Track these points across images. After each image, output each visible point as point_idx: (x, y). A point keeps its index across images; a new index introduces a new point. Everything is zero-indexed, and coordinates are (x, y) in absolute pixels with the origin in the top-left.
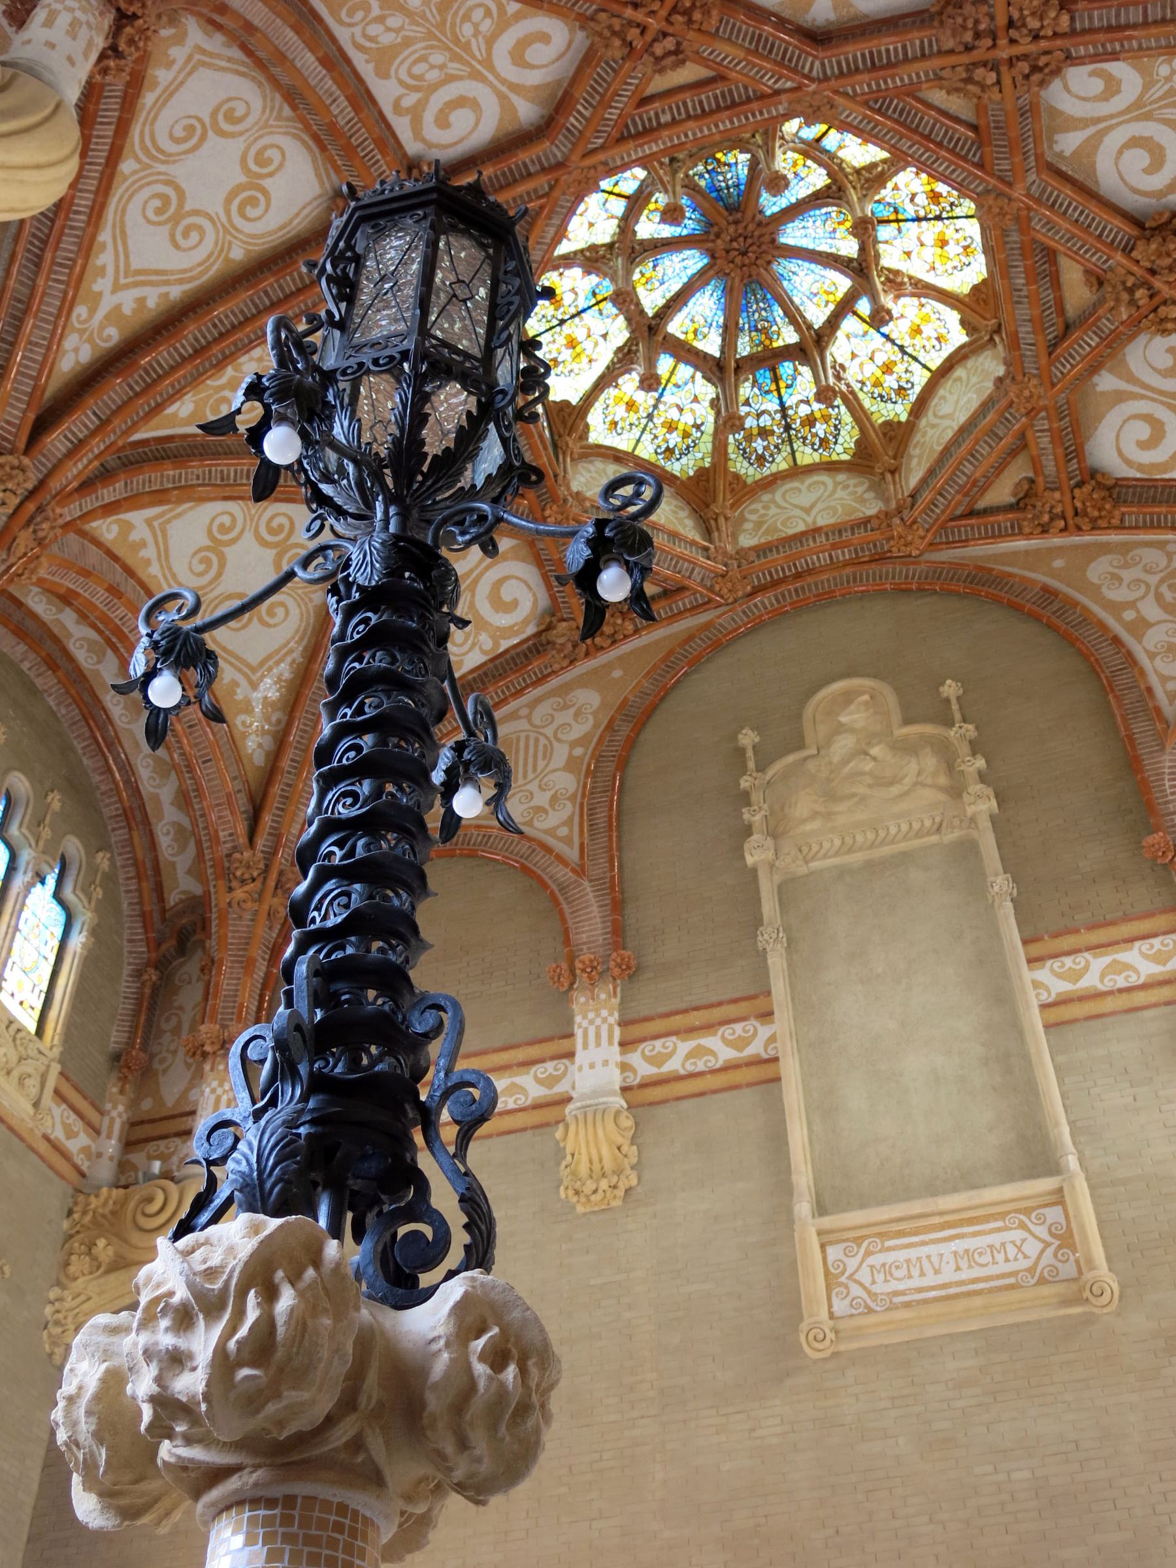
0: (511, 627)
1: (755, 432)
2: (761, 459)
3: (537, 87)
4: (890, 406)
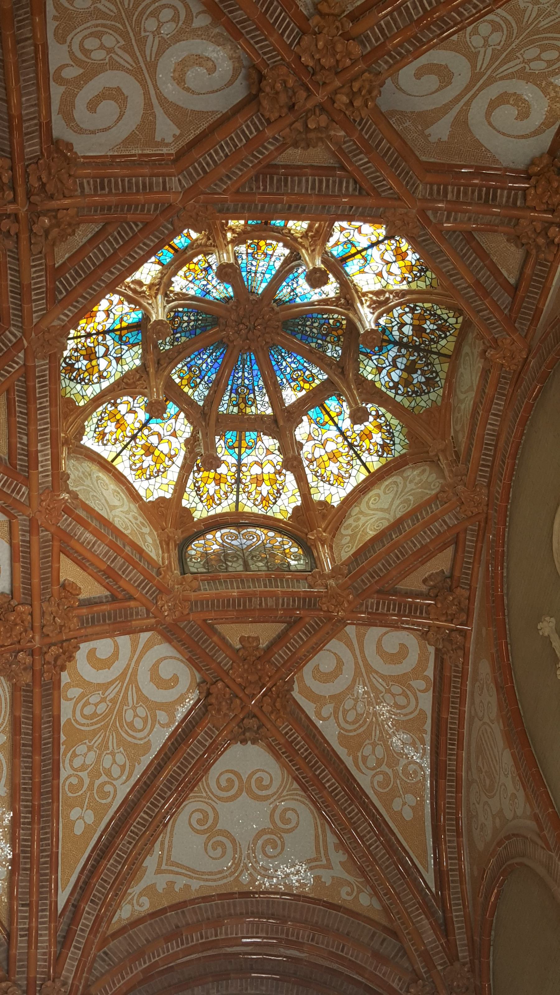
0: (420, 660)
1: (405, 375)
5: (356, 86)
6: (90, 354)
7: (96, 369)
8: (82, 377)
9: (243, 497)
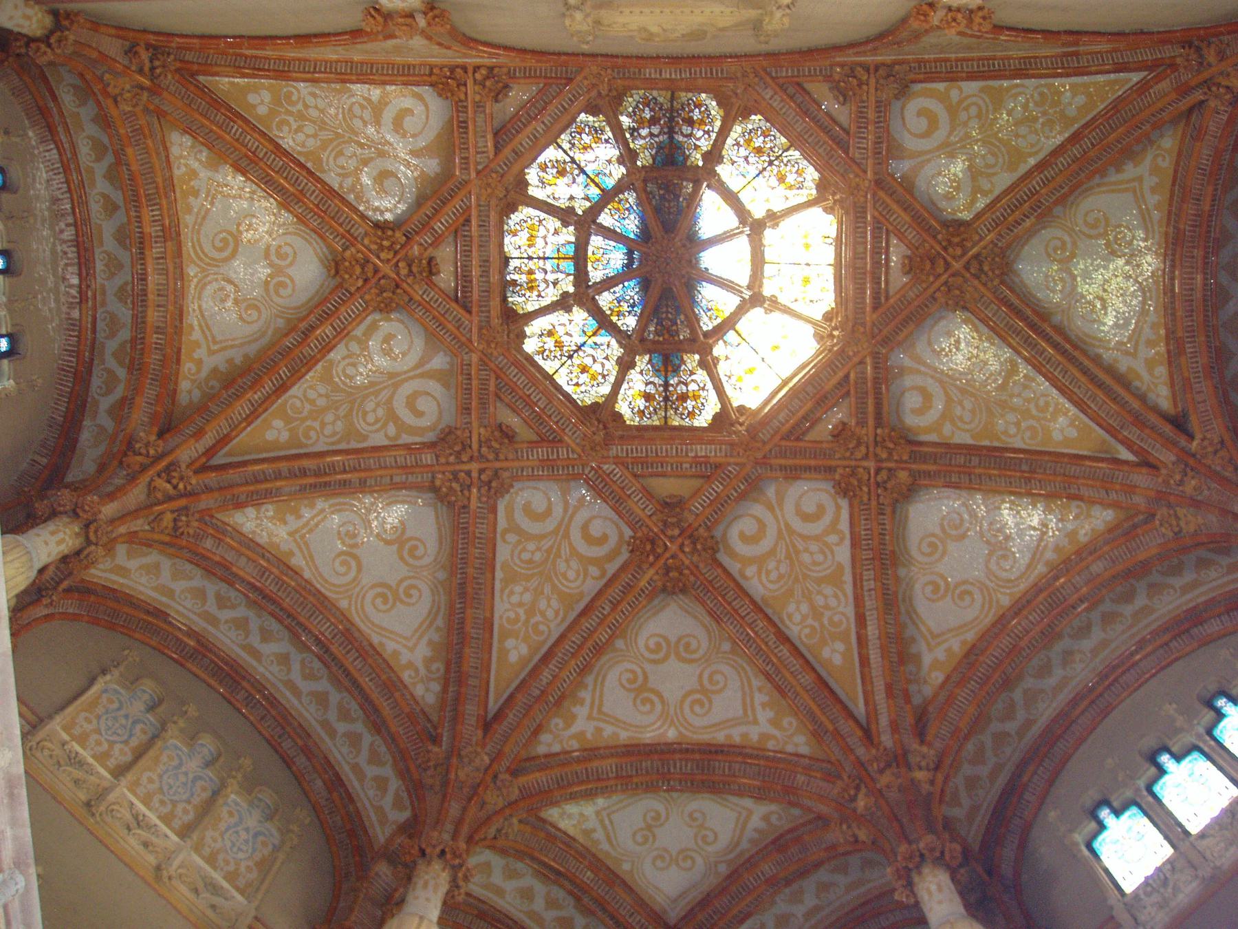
3: (756, 500)
5: (374, 247)
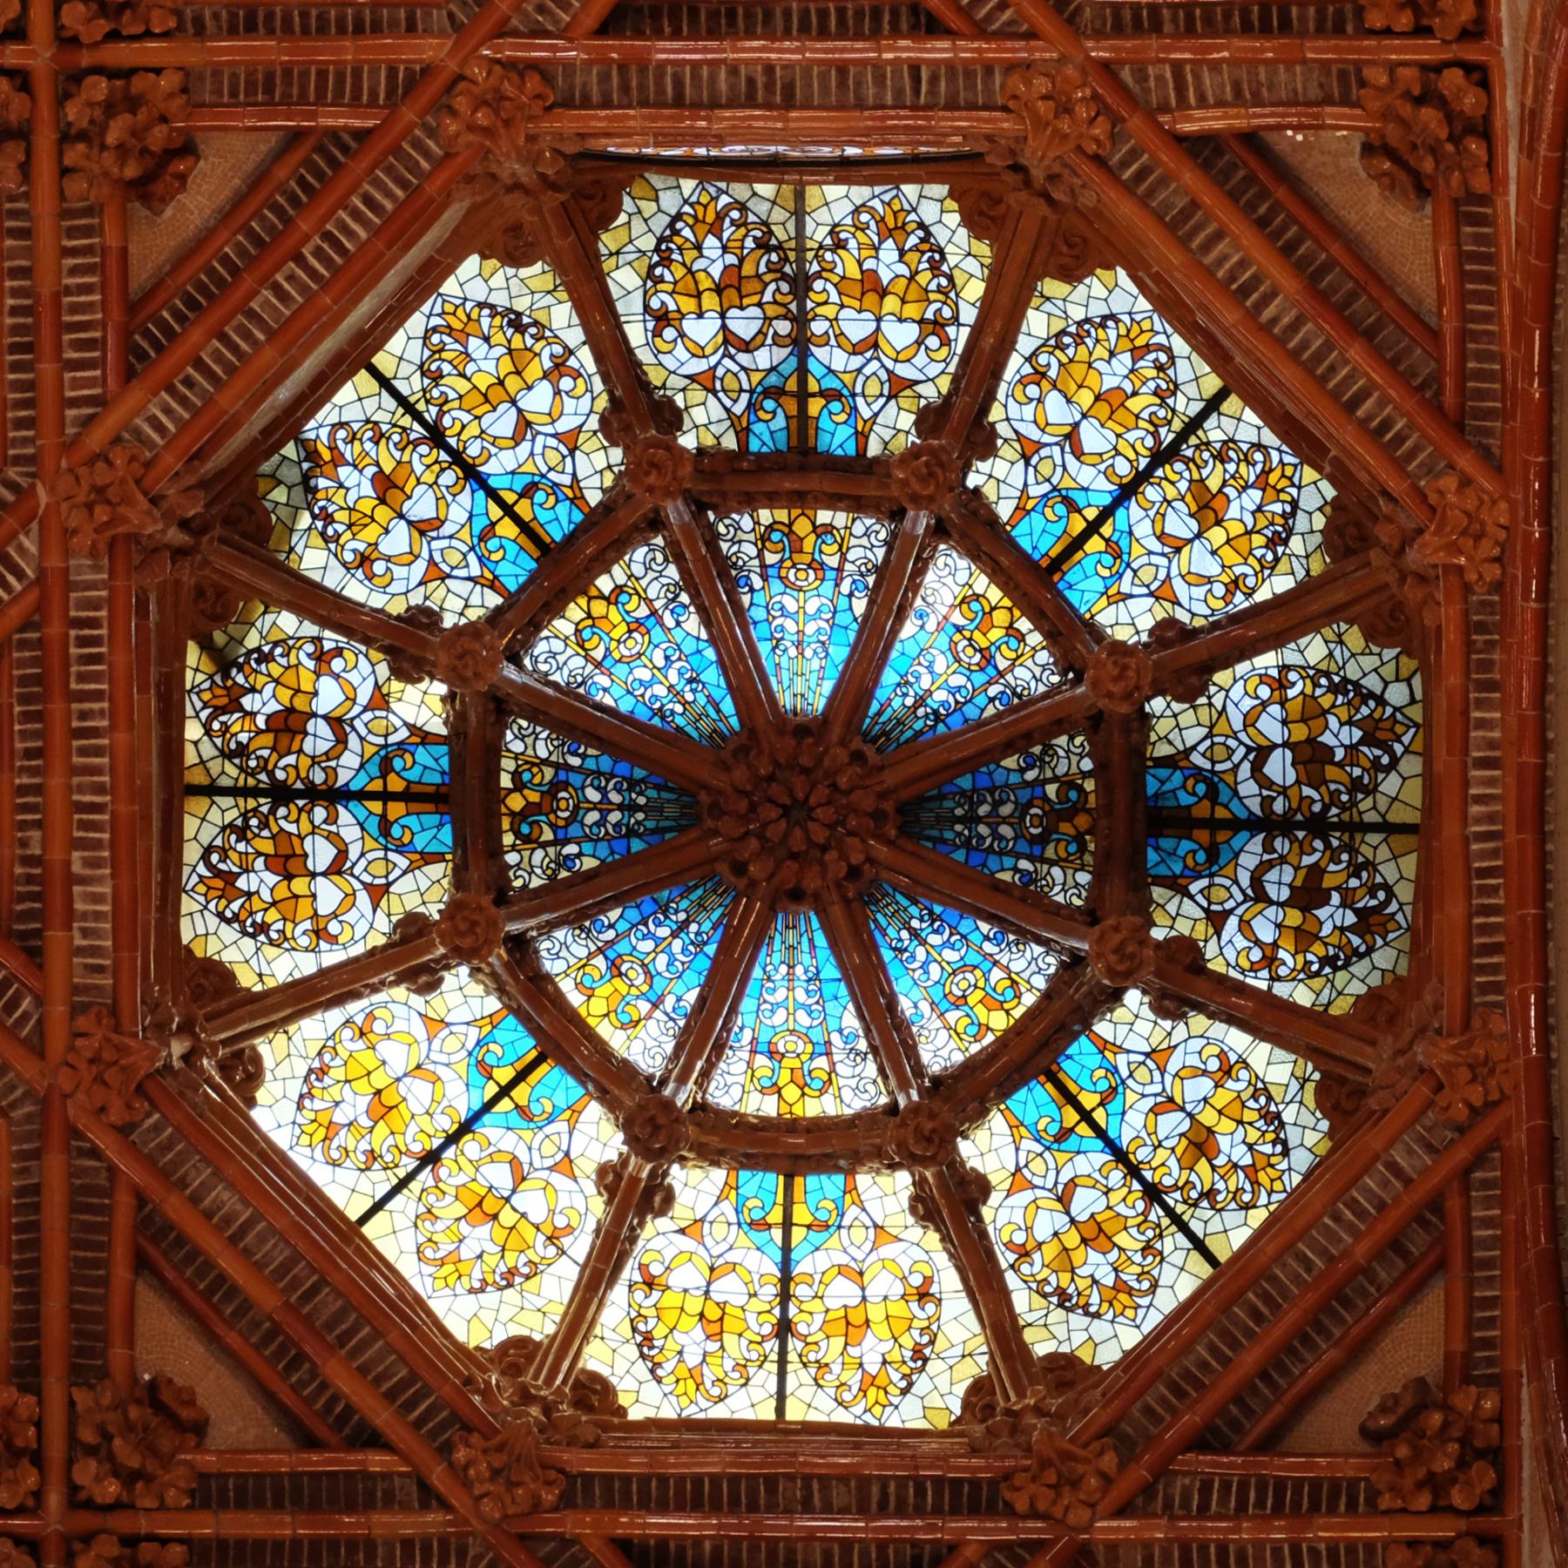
1: (1294, 917)
2: (1370, 923)
4: (1301, 522)
6: (288, 857)
7: (304, 907)
8: (258, 918)
9: (798, 1377)
